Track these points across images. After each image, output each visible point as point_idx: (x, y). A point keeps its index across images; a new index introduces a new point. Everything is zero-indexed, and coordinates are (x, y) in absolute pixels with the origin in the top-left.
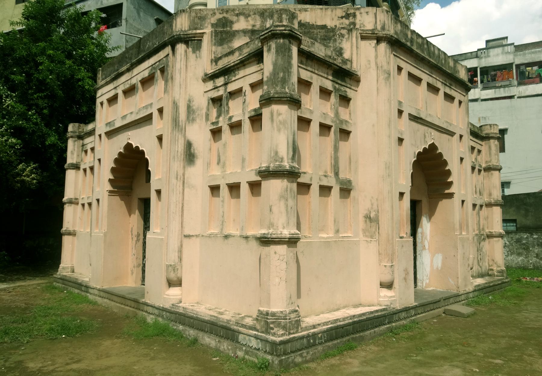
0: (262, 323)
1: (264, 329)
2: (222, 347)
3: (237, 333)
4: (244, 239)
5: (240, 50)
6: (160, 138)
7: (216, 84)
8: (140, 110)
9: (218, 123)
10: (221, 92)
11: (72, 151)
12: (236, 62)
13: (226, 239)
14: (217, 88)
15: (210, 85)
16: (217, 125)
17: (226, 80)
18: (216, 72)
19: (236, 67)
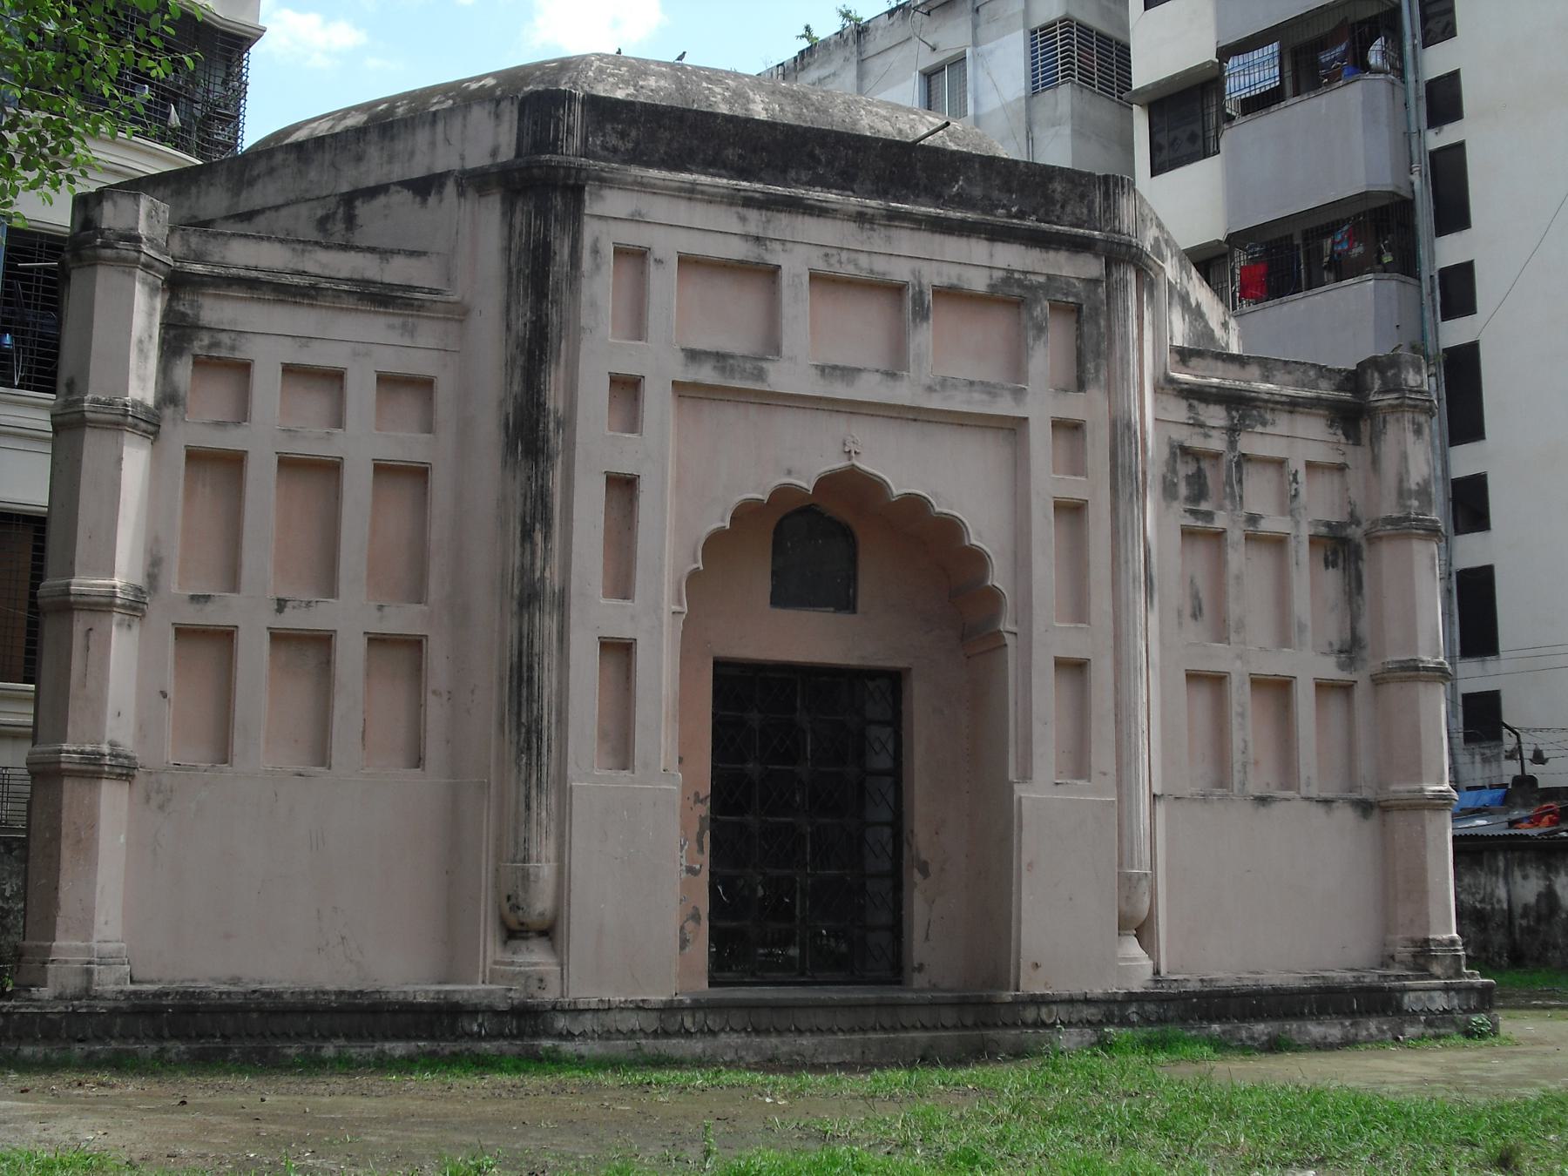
0: (1448, 962)
1: (1451, 972)
2: (1365, 1033)
3: (1398, 995)
4: (1320, 805)
5: (1265, 367)
6: (1071, 511)
7: (1202, 418)
8: (944, 382)
9: (1213, 519)
10: (1217, 443)
11: (140, 342)
12: (1277, 398)
13: (1264, 805)
14: (1202, 425)
15: (1178, 410)
16: (1207, 522)
17: (1236, 422)
18: (1208, 389)
19: (1271, 405)
